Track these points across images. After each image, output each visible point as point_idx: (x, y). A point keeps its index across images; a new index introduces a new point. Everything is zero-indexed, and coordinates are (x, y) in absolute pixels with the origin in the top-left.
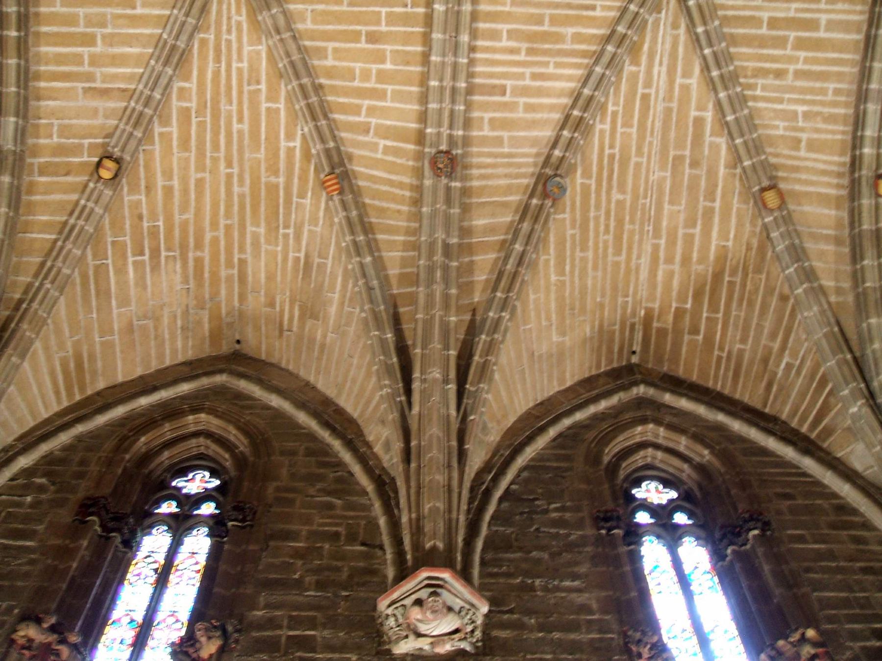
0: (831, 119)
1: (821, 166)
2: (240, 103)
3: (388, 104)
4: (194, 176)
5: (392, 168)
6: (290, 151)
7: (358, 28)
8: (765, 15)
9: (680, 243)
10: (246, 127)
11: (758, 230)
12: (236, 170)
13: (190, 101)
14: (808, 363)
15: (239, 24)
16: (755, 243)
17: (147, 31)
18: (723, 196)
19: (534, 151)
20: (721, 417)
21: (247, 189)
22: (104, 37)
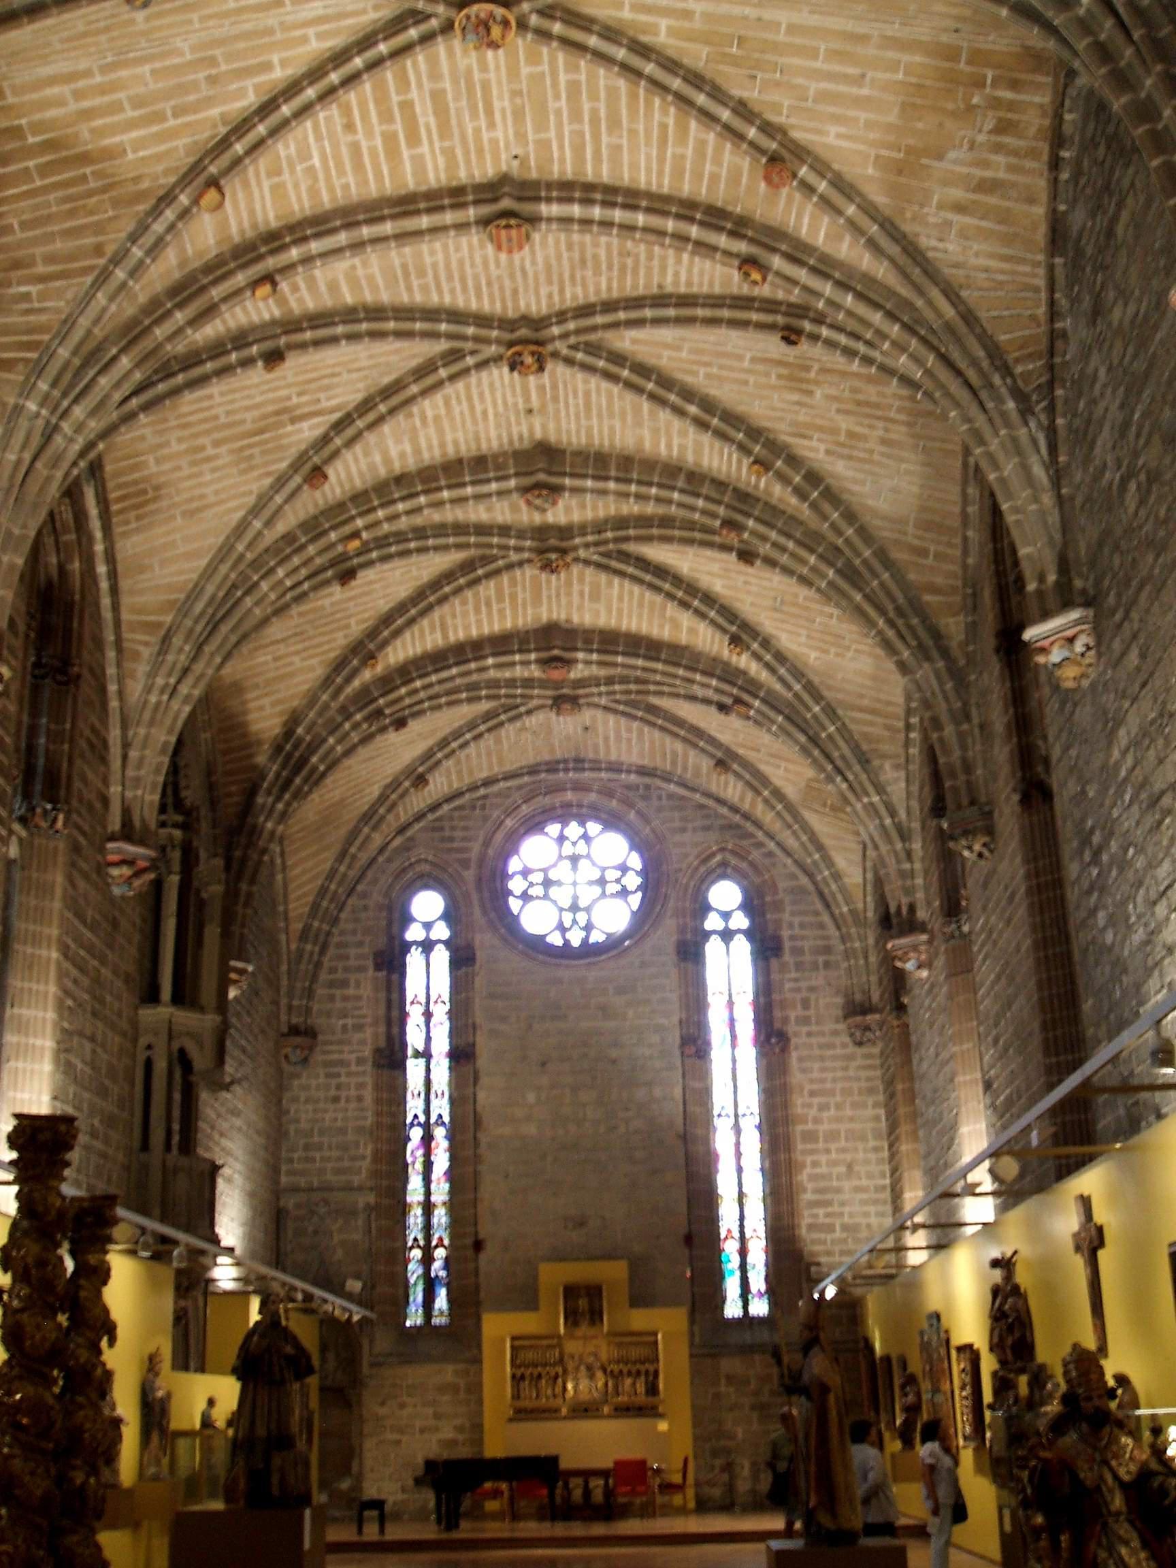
0: (314, 192)
1: (258, 207)
8: (414, 94)
9: (106, 99)
11: (162, 181)
14: (43, 318)
16: (145, 184)
18: (188, 125)
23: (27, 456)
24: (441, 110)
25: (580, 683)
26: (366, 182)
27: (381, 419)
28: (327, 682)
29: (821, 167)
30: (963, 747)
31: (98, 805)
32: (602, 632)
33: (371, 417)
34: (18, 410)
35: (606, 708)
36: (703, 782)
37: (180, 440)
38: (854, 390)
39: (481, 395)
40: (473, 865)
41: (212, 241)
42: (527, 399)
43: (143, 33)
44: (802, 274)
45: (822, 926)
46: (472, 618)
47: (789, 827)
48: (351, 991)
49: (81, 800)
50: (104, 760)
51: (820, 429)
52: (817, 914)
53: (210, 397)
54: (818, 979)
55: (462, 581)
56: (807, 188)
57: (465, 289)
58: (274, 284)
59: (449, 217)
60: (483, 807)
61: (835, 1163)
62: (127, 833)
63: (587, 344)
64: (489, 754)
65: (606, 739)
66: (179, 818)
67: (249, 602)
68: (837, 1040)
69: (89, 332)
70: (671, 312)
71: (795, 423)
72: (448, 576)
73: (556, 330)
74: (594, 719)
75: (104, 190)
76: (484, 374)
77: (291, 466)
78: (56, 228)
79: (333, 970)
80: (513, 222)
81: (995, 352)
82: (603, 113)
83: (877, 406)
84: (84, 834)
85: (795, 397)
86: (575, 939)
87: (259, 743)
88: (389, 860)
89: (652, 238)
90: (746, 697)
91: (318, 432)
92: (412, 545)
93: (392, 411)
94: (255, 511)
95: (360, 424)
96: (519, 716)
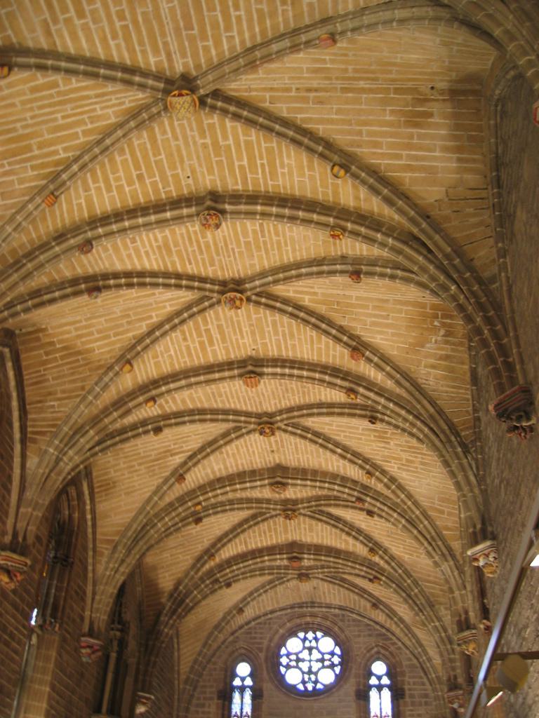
0: (172, 364)
1: (149, 371)
2: (74, 115)
3: (106, 196)
4: (17, 101)
5: (70, 211)
6: (56, 152)
7: (143, 168)
8: (210, 326)
10: (61, 122)
11: (109, 361)
12: (30, 122)
13: (64, 85)
15: (123, 103)
16: (102, 363)
17: (100, 50)
18: (119, 340)
19: (107, 266)
20: (14, 395)
21: (21, 132)
22: (87, 24)
23: (47, 471)
24: (222, 333)
25: (310, 568)
26: (193, 360)
27: (208, 455)
28: (194, 566)
29: (375, 351)
30: (463, 602)
31: (78, 620)
32: (315, 545)
33: (204, 454)
34: (46, 451)
35: (322, 579)
37: (124, 463)
38: (407, 442)
39: (251, 445)
41: (130, 384)
42: (271, 447)
43: (100, 306)
44: (372, 395)
45: (423, 684)
46: (258, 539)
48: (206, 709)
49: (69, 618)
50: (83, 600)
52: (421, 678)
53: (137, 445)
55: (252, 523)
56: (369, 360)
57: (239, 402)
58: (155, 402)
59: (227, 374)
60: (270, 624)
62: (91, 634)
63: (293, 423)
64: (272, 599)
65: (324, 593)
66: (120, 627)
67: (152, 531)
69: (76, 421)
70: (325, 410)
71: (383, 456)
72: (246, 521)
73: (278, 418)
75: (87, 364)
76: (251, 436)
77: (171, 474)
78: (66, 380)
79: (199, 699)
80: (252, 376)
81: (452, 427)
82: (287, 332)
84: (69, 633)
85: (383, 445)
86: (310, 687)
87: (163, 593)
89: (310, 381)
90: (379, 576)
91: (182, 460)
92: (228, 507)
93: (213, 451)
94: (155, 493)
95: (199, 457)
96: (283, 583)
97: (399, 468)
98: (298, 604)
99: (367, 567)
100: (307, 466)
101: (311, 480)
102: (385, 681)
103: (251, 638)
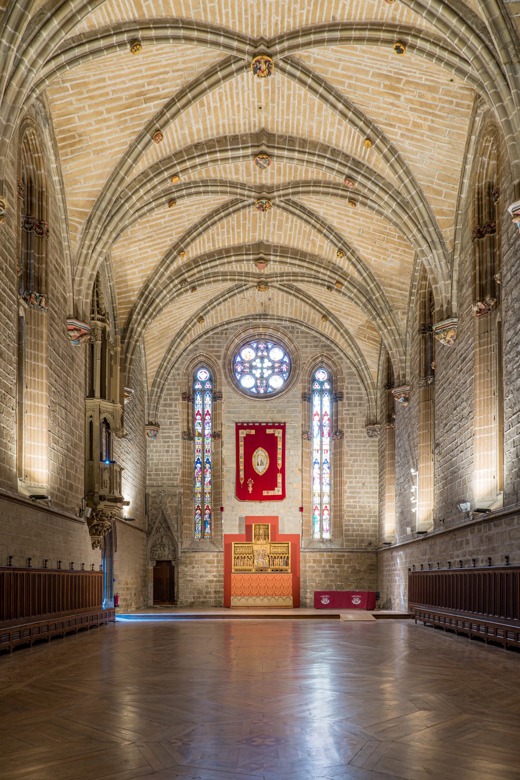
32: (281, 247)
36: (315, 326)
38: (421, 96)
39: (237, 94)
40: (222, 358)
42: (259, 101)
45: (359, 389)
47: (350, 346)
51: (400, 120)
52: (358, 384)
54: (356, 410)
55: (223, 214)
60: (226, 334)
61: (358, 482)
68: (362, 435)
71: (388, 117)
74: (273, 294)
77: (145, 129)
83: (430, 106)
88: (188, 355)
91: (158, 109)
93: (194, 98)
95: (179, 105)
96: (243, 291)
97: (402, 135)
98: (253, 315)
99: (331, 271)
100: (295, 135)
101: (299, 152)
102: (327, 386)
103: (210, 347)
